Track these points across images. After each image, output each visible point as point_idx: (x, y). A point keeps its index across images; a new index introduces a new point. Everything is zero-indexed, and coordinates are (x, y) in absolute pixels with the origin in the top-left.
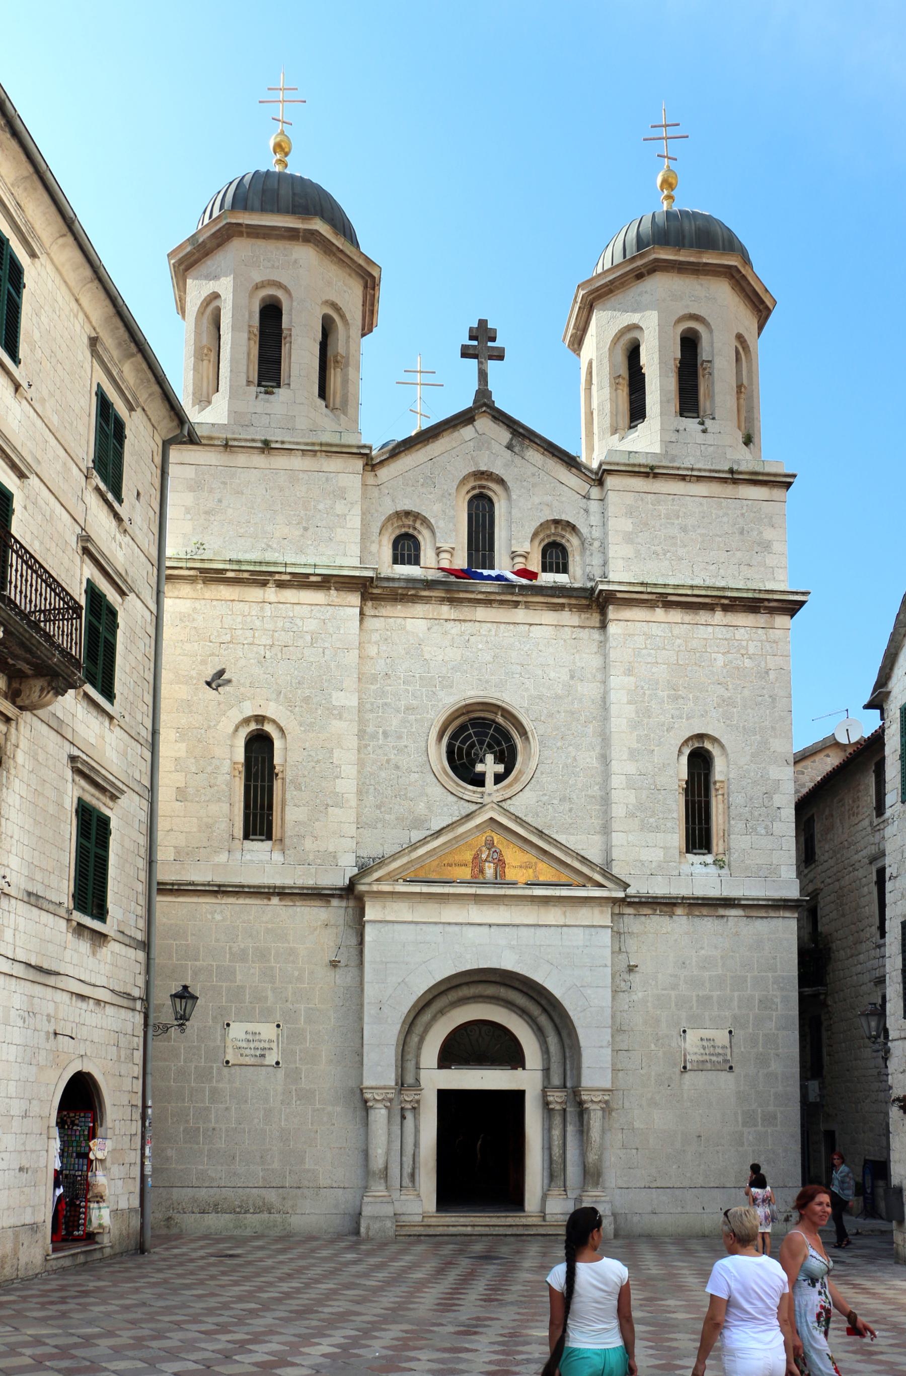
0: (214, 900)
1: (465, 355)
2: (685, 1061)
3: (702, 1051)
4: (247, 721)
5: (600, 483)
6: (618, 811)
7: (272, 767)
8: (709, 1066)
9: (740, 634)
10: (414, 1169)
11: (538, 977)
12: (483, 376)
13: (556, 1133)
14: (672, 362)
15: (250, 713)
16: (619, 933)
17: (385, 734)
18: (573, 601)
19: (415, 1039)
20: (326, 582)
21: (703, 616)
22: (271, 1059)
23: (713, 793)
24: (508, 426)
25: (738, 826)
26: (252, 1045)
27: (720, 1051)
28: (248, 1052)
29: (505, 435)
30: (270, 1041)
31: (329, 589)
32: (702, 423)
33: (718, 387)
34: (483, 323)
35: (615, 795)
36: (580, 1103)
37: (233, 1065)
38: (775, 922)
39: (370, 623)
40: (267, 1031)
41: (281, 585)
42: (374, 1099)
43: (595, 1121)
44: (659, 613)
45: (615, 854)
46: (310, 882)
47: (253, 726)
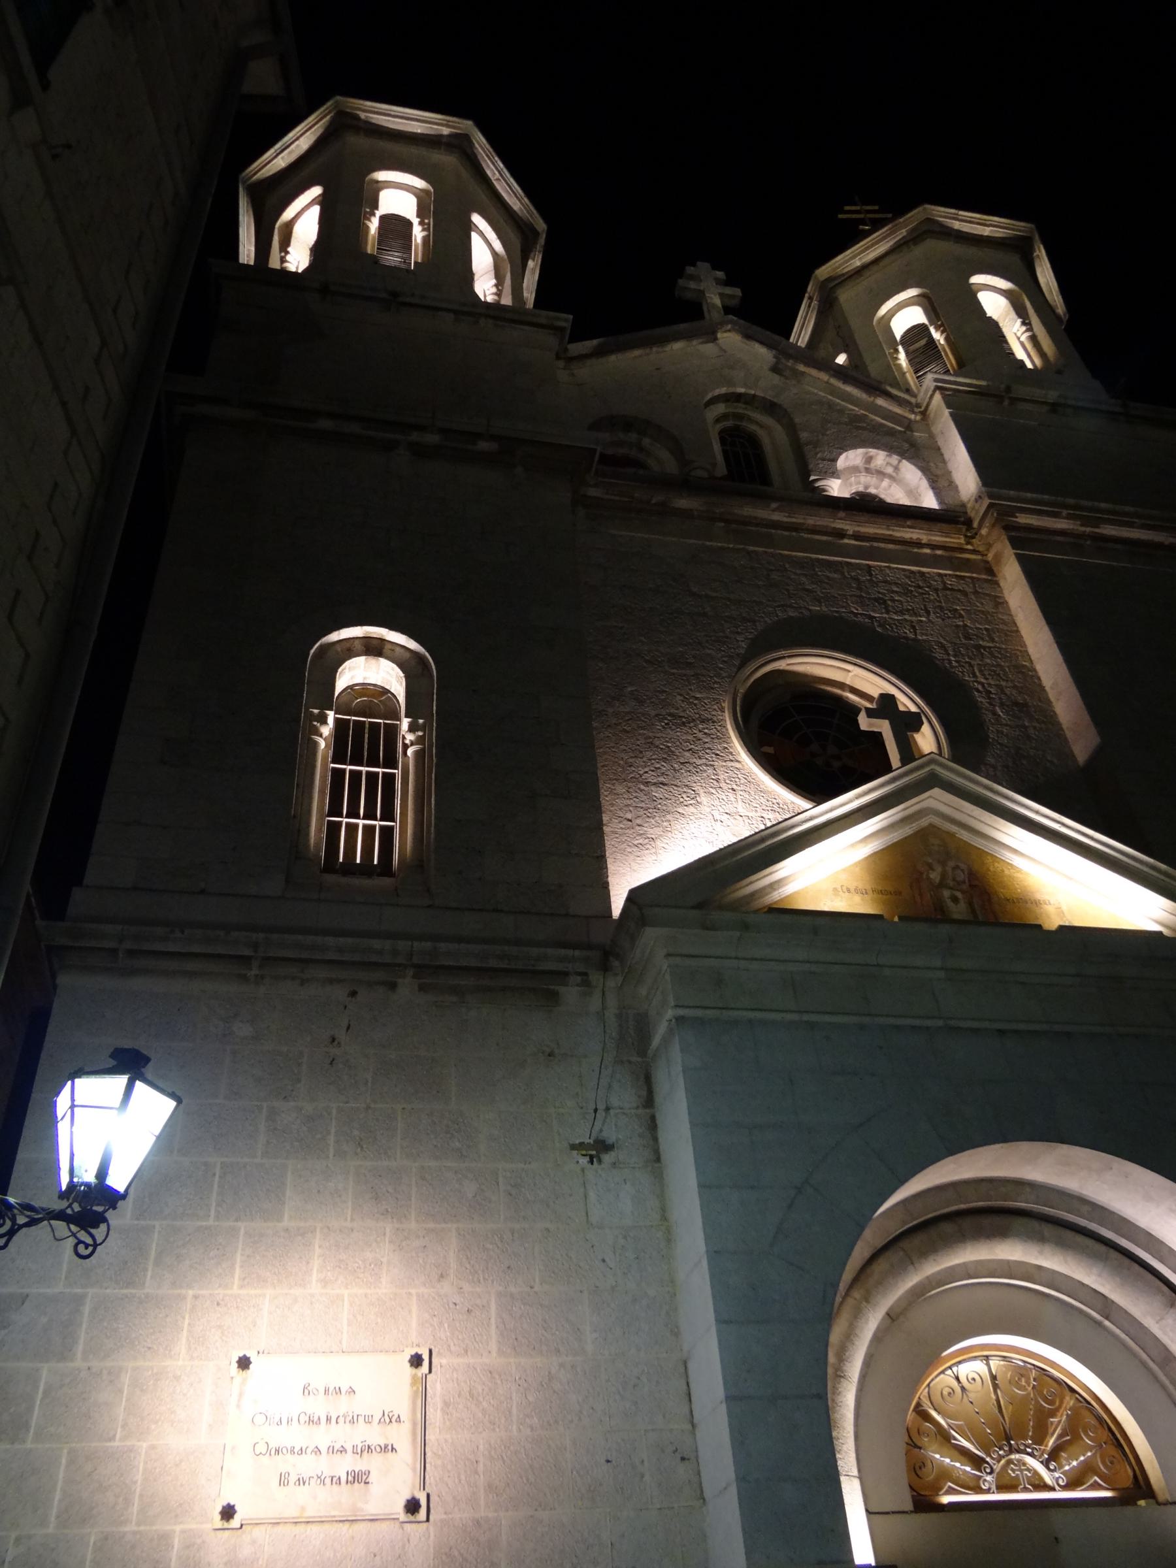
26: (323, 1437)
28: (307, 1465)
30: (389, 1419)
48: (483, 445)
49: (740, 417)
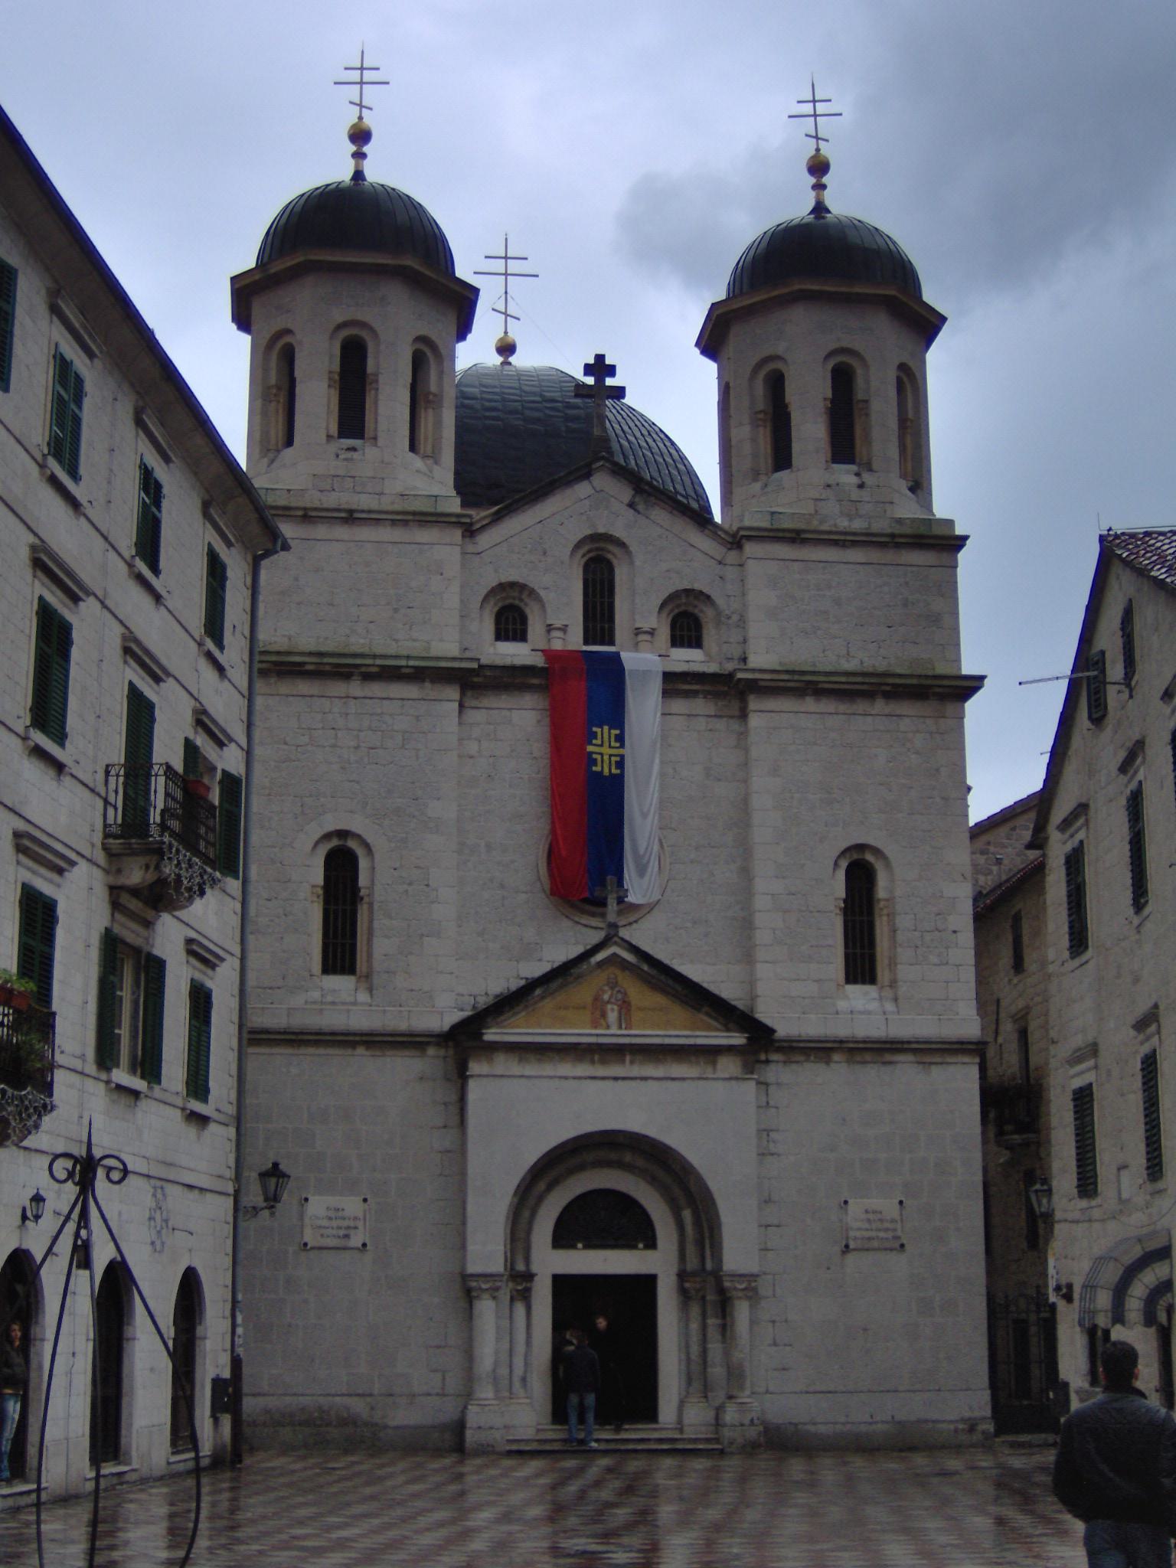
0: (289, 1051)
2: (847, 1238)
3: (867, 1226)
4: (327, 836)
6: (762, 936)
7: (355, 889)
8: (875, 1244)
9: (905, 724)
10: (526, 1372)
11: (671, 1140)
13: (694, 1326)
14: (822, 404)
15: (331, 827)
16: (767, 1084)
17: (488, 846)
18: (707, 688)
19: (526, 1214)
21: (861, 706)
22: (356, 1241)
23: (877, 911)
25: (904, 954)
27: (887, 1225)
28: (329, 1232)
29: (626, 493)
30: (356, 1218)
31: (423, 681)
32: (858, 474)
33: (876, 433)
34: (600, 358)
35: (760, 919)
36: (721, 1291)
37: (312, 1248)
38: (952, 1068)
39: (472, 716)
40: (352, 1206)
42: (480, 1289)
43: (742, 1312)
44: (810, 704)
45: (761, 988)
46: (403, 1026)
47: (335, 842)
48: (404, 671)
49: (602, 549)
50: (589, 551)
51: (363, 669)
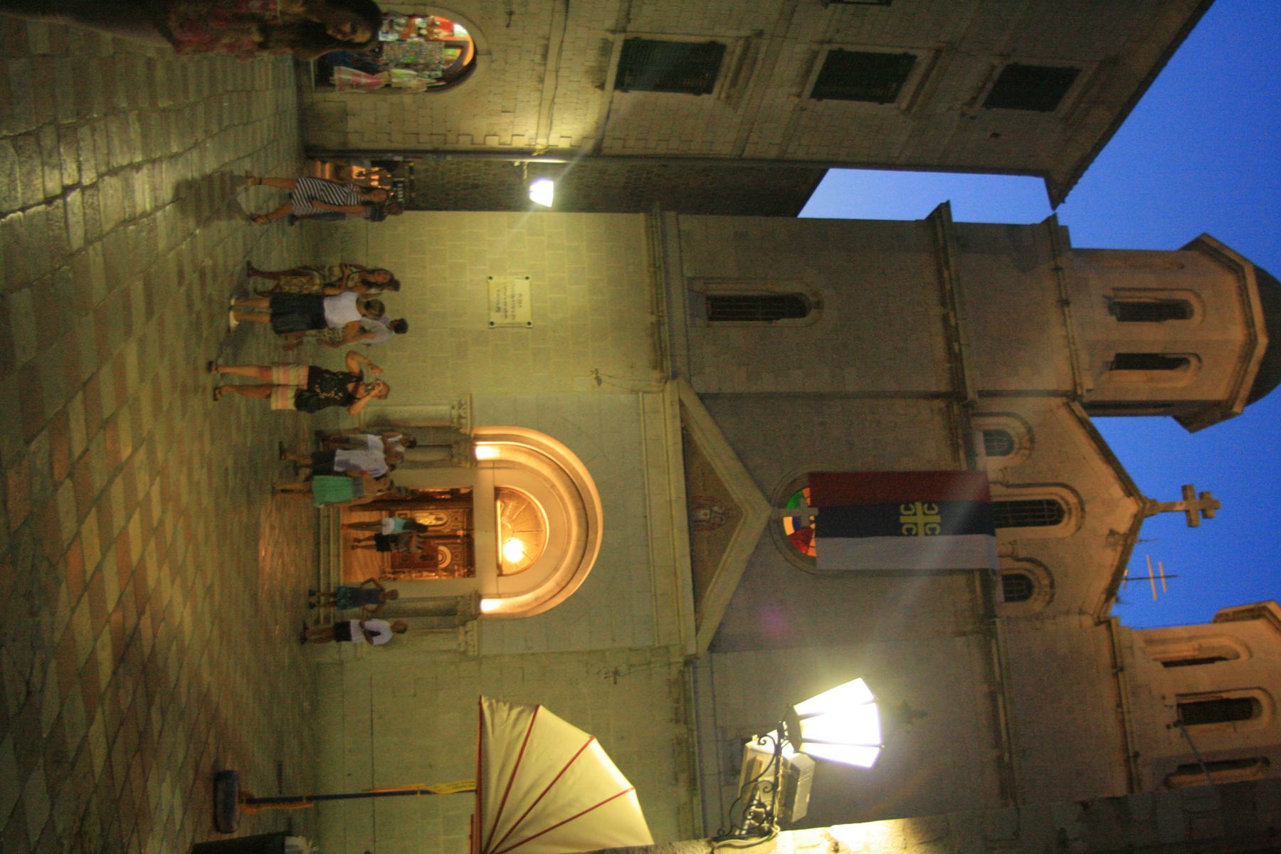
1: (1184, 488)
5: (1098, 623)
12: (1169, 508)
18: (980, 602)
20: (955, 358)
24: (1130, 530)
30: (514, 317)
41: (945, 319)
48: (956, 346)
49: (1070, 513)
50: (1067, 503)
51: (951, 314)
